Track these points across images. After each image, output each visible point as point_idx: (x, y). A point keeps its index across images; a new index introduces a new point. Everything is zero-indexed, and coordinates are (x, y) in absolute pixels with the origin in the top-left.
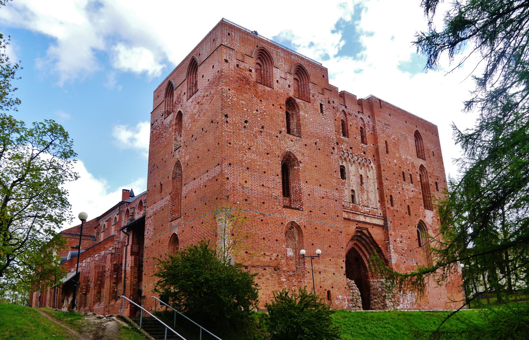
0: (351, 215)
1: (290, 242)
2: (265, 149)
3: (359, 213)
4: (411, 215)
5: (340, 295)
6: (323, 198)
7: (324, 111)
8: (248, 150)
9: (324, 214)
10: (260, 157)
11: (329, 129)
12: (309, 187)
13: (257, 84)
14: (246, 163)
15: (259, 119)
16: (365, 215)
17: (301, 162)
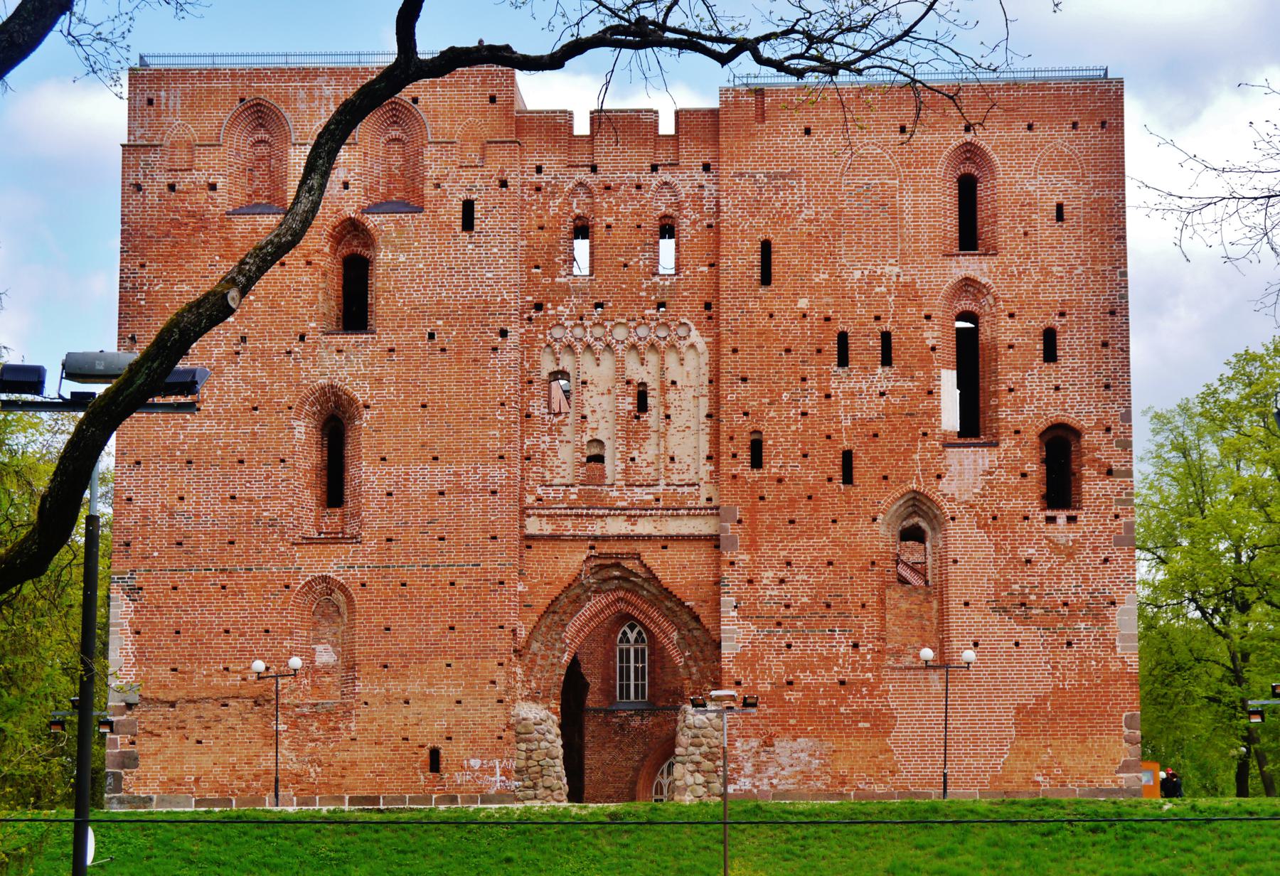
0: (569, 523)
1: (326, 630)
2: (246, 399)
3: (601, 512)
4: (856, 482)
5: (473, 757)
6: (442, 493)
7: (476, 222)
9: (442, 539)
11: (489, 275)
12: (390, 474)
13: (229, 220)
14: (183, 451)
16: (632, 512)
17: (367, 407)
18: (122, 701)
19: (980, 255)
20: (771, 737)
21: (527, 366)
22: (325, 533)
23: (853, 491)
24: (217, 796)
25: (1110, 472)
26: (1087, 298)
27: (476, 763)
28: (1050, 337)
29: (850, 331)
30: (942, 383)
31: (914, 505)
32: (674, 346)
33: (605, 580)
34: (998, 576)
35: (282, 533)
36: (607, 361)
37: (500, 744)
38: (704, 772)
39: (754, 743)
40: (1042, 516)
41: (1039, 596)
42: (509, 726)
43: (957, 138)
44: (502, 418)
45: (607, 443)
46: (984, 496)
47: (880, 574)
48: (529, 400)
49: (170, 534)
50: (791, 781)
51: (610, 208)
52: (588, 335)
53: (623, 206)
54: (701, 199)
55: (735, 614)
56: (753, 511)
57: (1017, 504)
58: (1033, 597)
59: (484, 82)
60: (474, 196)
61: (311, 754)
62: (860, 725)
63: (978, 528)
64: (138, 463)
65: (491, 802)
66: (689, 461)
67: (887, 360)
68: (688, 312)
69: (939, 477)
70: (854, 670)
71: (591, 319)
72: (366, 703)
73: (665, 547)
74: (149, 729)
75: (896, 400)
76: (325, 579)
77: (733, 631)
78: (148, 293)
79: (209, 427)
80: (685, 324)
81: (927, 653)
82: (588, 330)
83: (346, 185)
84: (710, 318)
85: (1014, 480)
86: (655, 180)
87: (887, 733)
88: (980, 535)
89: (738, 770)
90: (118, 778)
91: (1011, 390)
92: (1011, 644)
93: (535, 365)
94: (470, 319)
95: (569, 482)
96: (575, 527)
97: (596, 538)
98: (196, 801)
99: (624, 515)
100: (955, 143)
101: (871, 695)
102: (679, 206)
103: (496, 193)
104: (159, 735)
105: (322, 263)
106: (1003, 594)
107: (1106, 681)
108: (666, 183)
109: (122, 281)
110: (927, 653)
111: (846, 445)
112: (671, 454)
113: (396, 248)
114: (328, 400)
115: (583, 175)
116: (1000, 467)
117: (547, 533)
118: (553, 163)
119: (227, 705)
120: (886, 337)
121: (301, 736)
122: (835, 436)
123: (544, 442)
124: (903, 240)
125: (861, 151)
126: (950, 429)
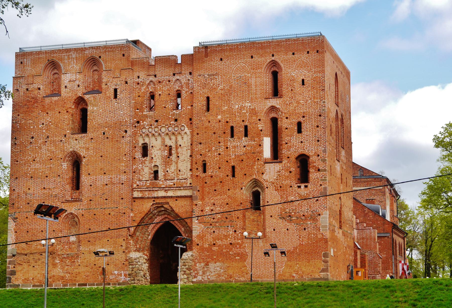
0: (147, 193)
2: (48, 156)
3: (156, 189)
4: (236, 176)
5: (115, 270)
6: (107, 185)
7: (118, 96)
8: (33, 162)
9: (106, 199)
10: (43, 165)
11: (122, 113)
12: (91, 179)
13: (44, 99)
14: (30, 174)
15: (44, 131)
17: (84, 157)
18: (11, 254)
19: (278, 98)
20: (208, 262)
21: (134, 142)
22: (73, 199)
23: (235, 179)
24: (39, 284)
25: (319, 170)
26: (311, 111)
27: (116, 272)
28: (299, 125)
29: (234, 125)
30: (264, 142)
31: (256, 183)
32: (180, 133)
33: (160, 211)
34: (281, 207)
35: (59, 199)
36: (159, 139)
37: (123, 266)
38: (187, 274)
39: (203, 264)
40: (296, 186)
41: (295, 213)
42: (127, 260)
43: (269, 59)
44: (125, 159)
45: (159, 166)
46: (277, 180)
48: (135, 153)
49: (26, 200)
50: (214, 277)
52: (153, 131)
53: (164, 88)
55: (197, 222)
56: (203, 187)
57: (288, 182)
58: (293, 213)
59: (121, 50)
60: (117, 87)
61: (67, 270)
62: (237, 258)
63: (275, 190)
64: (17, 178)
65: (120, 285)
66: (185, 171)
67: (246, 135)
68: (184, 122)
69: (263, 174)
70: (235, 239)
71: (154, 126)
72: (83, 253)
73: (176, 200)
74: (19, 263)
75: (249, 148)
76: (71, 213)
77: (196, 227)
78: (20, 124)
79: (37, 166)
80: (183, 126)
81: (260, 234)
82: (153, 129)
83: (79, 86)
84: (191, 123)
85: (287, 174)
86: (174, 79)
87: (245, 261)
89: (197, 274)
90: (10, 279)
91: (286, 143)
92: (286, 230)
93: (137, 141)
94: (116, 127)
95: (147, 180)
96: (149, 194)
97: (155, 198)
98: (33, 285)
99: (164, 190)
100: (269, 61)
101: (240, 248)
102: (182, 87)
103: (124, 86)
104: (22, 265)
105: (71, 112)
106: (284, 213)
107: (317, 241)
108: (178, 79)
109: (13, 120)
110: (260, 234)
111: (233, 164)
112: (179, 169)
113: (94, 105)
114: (74, 156)
115: (152, 78)
116: (283, 169)
117: (140, 196)
118: (142, 75)
119: (42, 255)
120: (246, 127)
121: (64, 264)
122: (229, 161)
123: (140, 167)
124: (252, 94)
125: (238, 65)
126: (267, 157)
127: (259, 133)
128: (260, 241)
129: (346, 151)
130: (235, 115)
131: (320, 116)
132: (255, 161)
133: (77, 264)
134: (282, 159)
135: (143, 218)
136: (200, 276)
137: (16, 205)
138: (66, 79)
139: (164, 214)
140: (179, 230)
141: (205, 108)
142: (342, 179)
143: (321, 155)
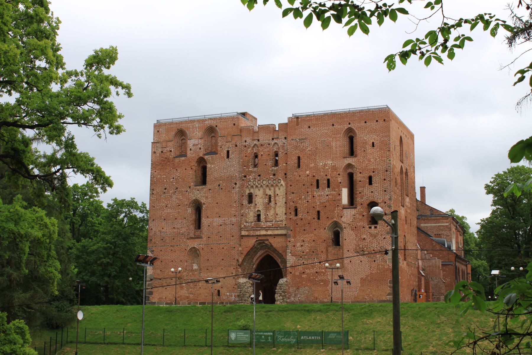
0: (252, 232)
2: (177, 203)
4: (320, 219)
6: (221, 225)
9: (221, 237)
16: (267, 229)
23: (320, 221)
24: (170, 302)
27: (228, 294)
28: (370, 178)
35: (185, 236)
38: (282, 296)
40: (368, 227)
41: (367, 248)
42: (236, 284)
45: (261, 211)
47: (326, 243)
51: (262, 150)
54: (284, 146)
55: (290, 255)
57: (361, 224)
58: (365, 249)
59: (232, 120)
66: (281, 215)
67: (328, 187)
68: (280, 176)
69: (341, 217)
70: (320, 269)
76: (194, 248)
77: (290, 259)
78: (156, 178)
79: (169, 210)
83: (200, 149)
84: (286, 177)
85: (361, 217)
87: (328, 286)
88: (352, 232)
90: (149, 297)
91: (360, 193)
92: (360, 261)
93: (245, 192)
96: (253, 233)
97: (258, 235)
100: (346, 128)
102: (279, 148)
108: (276, 143)
110: (338, 265)
111: (318, 209)
113: (211, 164)
114: (196, 203)
115: (256, 142)
116: (357, 214)
120: (328, 180)
122: (315, 207)
127: (339, 186)
128: (340, 270)
129: (410, 199)
130: (320, 170)
131: (387, 171)
132: (335, 207)
133: (199, 287)
134: (356, 205)
135: (249, 251)
136: (292, 297)
137: (153, 241)
138: (191, 143)
139: (265, 249)
140: (277, 261)
141: (296, 165)
142: (406, 221)
143: (388, 202)
